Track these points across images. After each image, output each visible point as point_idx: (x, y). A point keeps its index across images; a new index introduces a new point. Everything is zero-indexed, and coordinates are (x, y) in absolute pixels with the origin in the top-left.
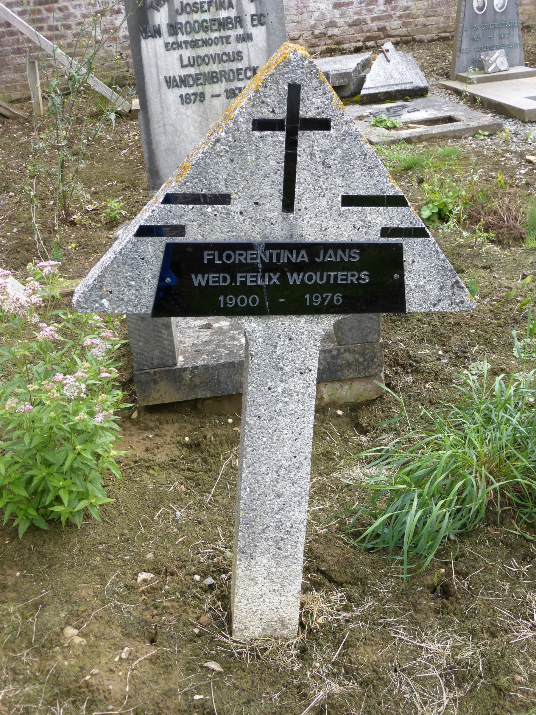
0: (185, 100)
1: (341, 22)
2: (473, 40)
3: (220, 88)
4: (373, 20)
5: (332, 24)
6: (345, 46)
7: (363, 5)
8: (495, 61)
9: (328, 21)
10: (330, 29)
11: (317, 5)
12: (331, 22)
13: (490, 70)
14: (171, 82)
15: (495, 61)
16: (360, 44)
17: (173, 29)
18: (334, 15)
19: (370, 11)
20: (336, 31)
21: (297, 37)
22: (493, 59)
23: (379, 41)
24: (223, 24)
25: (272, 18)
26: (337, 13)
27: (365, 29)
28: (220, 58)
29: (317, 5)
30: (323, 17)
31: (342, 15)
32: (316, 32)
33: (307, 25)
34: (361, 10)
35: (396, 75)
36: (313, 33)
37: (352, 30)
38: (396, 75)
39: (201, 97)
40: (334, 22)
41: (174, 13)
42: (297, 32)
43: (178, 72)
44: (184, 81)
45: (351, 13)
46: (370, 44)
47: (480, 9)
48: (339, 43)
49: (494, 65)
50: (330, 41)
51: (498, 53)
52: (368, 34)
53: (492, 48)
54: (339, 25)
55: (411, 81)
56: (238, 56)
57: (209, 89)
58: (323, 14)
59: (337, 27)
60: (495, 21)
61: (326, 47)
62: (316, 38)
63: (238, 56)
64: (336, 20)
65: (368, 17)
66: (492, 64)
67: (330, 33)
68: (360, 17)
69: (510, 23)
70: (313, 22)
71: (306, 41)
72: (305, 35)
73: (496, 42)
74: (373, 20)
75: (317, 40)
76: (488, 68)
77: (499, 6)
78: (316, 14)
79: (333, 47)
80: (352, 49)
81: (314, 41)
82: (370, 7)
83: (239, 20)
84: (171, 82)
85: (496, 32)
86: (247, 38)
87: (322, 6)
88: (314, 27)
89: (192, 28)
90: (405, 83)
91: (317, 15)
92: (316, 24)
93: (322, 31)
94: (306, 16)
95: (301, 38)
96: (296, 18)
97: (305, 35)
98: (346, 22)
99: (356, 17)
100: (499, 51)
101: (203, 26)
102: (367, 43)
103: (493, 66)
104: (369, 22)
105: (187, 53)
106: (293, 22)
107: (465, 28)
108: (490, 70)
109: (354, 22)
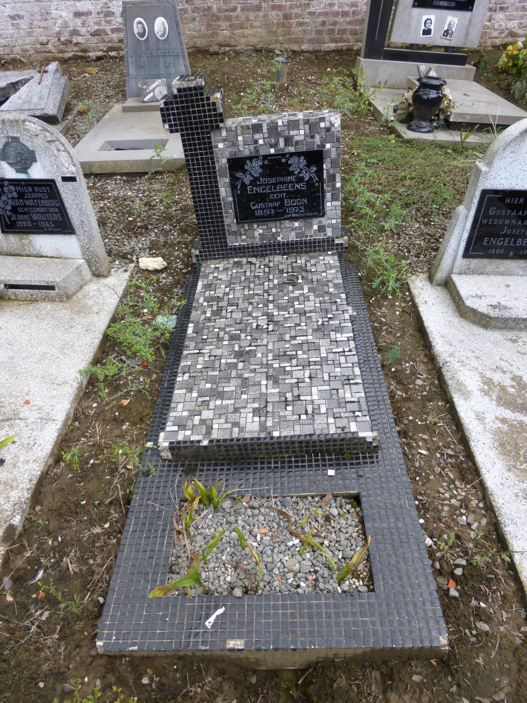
1: (83, 30)
2: (139, 67)
4: (113, 31)
5: (75, 32)
6: (90, 54)
7: (101, 16)
8: (153, 91)
9: (72, 29)
10: (74, 37)
11: (59, 13)
12: (74, 30)
13: (146, 99)
15: (153, 91)
16: (100, 54)
18: (76, 23)
19: (108, 22)
20: (80, 39)
21: (45, 42)
22: (151, 88)
23: (120, 52)
26: (78, 22)
27: (106, 40)
29: (59, 13)
30: (65, 25)
31: (83, 24)
32: (63, 39)
33: (53, 31)
34: (100, 21)
35: (35, 100)
36: (59, 39)
37: (95, 40)
38: (35, 100)
40: (77, 30)
42: (44, 37)
45: (92, 24)
46: (113, 54)
47: (142, 35)
48: (84, 51)
49: (151, 94)
50: (76, 49)
51: (158, 82)
52: (110, 44)
53: (157, 77)
54: (82, 33)
55: (43, 107)
58: (65, 22)
59: (80, 36)
60: (158, 49)
61: (74, 53)
62: (63, 44)
64: (79, 29)
65: (108, 28)
66: (150, 93)
67: (75, 41)
68: (100, 28)
69: (174, 52)
70: (58, 29)
71: (55, 46)
72: (53, 41)
73: (162, 70)
74: (113, 31)
75: (64, 46)
76: (145, 97)
77: (160, 33)
78: (60, 22)
79: (80, 54)
80: (94, 58)
81: (62, 47)
82: (108, 19)
85: (161, 60)
87: (64, 14)
88: (59, 34)
90: (37, 109)
91: (60, 22)
92: (60, 30)
93: (68, 38)
94: (50, 22)
95: (50, 43)
96: (42, 24)
97: (53, 41)
98: (88, 32)
99: (96, 28)
100: (160, 80)
102: (110, 53)
103: (151, 94)
104: (109, 33)
106: (40, 27)
107: (129, 55)
108: (146, 99)
109: (95, 31)
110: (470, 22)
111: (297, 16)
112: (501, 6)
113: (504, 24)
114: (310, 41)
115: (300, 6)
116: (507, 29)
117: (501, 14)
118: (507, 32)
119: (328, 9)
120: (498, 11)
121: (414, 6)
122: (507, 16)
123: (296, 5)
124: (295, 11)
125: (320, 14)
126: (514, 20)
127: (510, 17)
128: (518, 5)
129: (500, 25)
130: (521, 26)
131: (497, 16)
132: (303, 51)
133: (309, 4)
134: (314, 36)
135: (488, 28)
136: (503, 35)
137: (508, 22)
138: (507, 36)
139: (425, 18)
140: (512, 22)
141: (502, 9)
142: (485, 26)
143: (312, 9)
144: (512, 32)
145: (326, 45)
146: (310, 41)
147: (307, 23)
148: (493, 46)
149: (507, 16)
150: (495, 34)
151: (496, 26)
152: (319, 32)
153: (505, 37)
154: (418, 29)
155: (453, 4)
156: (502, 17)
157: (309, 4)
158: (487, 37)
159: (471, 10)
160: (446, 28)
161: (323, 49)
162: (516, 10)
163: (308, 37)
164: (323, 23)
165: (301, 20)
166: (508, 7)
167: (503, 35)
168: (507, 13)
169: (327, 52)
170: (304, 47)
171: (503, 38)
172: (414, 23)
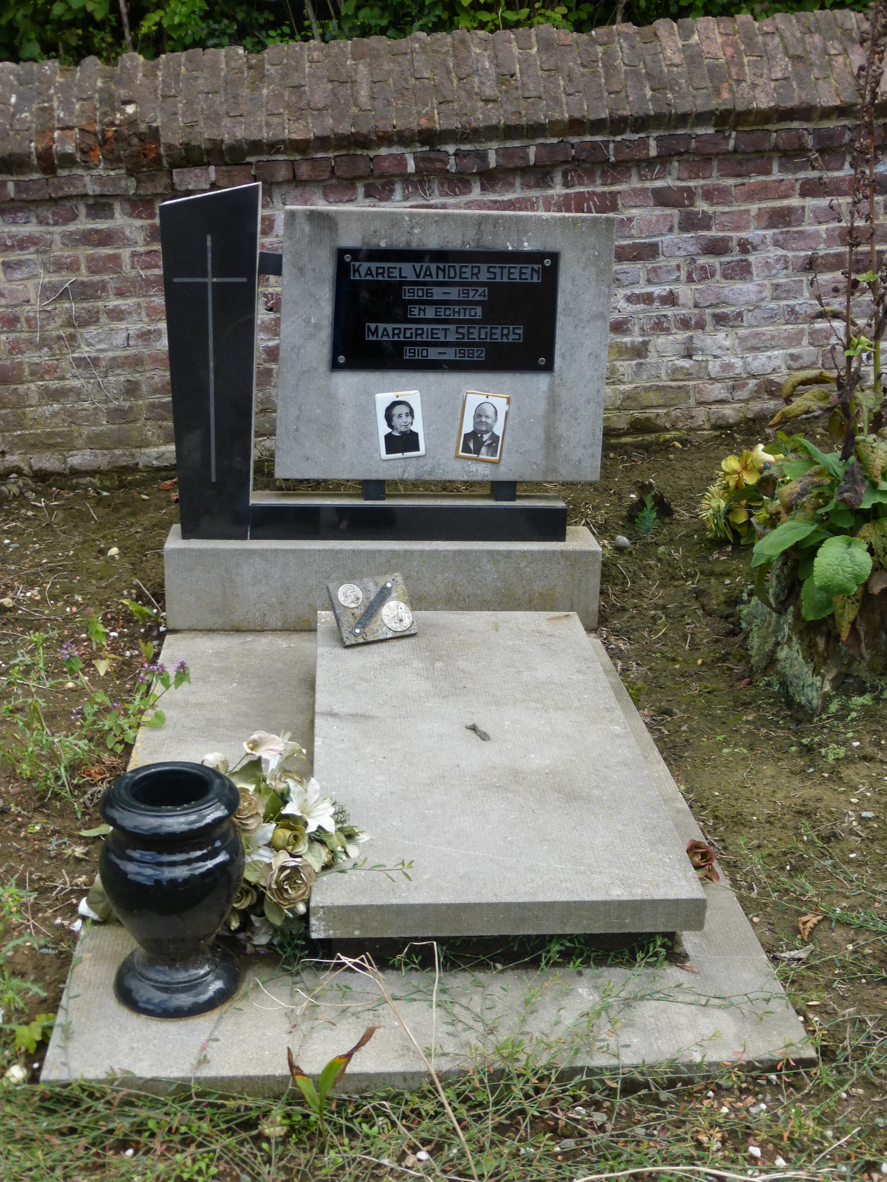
110: (553, 401)
111: (38, 373)
112: (718, 311)
113: (738, 363)
114: (95, 442)
115: (44, 343)
116: (754, 376)
117: (721, 335)
118: (752, 383)
119: (137, 349)
120: (709, 328)
121: (335, 366)
122: (742, 340)
123: (30, 342)
124: (30, 357)
125: (115, 364)
126: (767, 348)
127: (754, 342)
128: (773, 305)
129: (728, 367)
130: (795, 365)
131: (709, 341)
132: (75, 472)
133: (72, 337)
134: (104, 426)
135: (689, 375)
136: (743, 394)
137: (750, 357)
138: (756, 395)
139: (383, 399)
140: (762, 357)
141: (720, 320)
142: (676, 370)
143: (85, 351)
144: (771, 382)
145: (153, 451)
146: (95, 442)
147: (77, 393)
148: (715, 427)
149: (742, 340)
150: (717, 391)
151: (714, 368)
152: (119, 415)
153: (752, 398)
154: (367, 432)
155: (478, 355)
156: (727, 343)
157: (72, 337)
158: (692, 402)
159: (549, 368)
160: (468, 427)
161: (142, 462)
162: (771, 318)
163: (85, 431)
164: (131, 389)
165: (54, 384)
166: (740, 315)
167: (743, 394)
168: (742, 332)
169: (158, 469)
170: (79, 459)
171: (746, 401)
172: (347, 416)
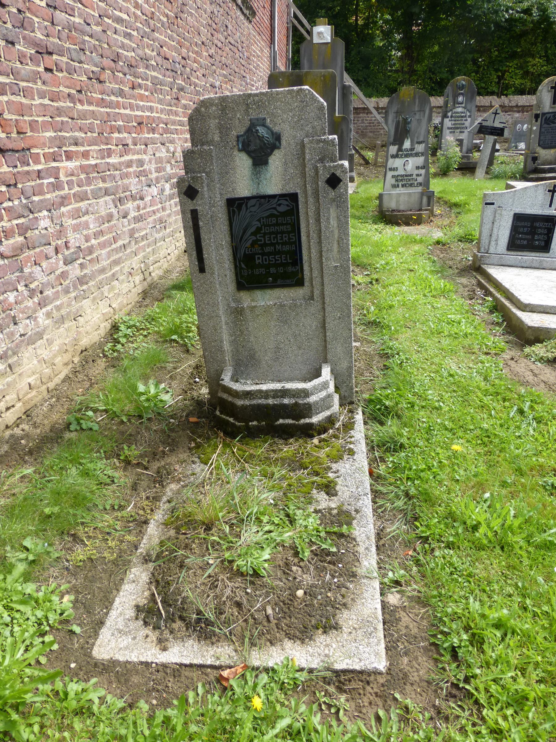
0: (451, 132)
3: (458, 130)
14: (448, 128)
17: (452, 117)
24: (462, 117)
25: (472, 116)
28: (460, 124)
39: (454, 132)
41: (452, 113)
43: (450, 126)
44: (451, 128)
53: (521, 142)
56: (464, 124)
57: (456, 131)
63: (464, 124)
83: (466, 116)
84: (448, 128)
86: (466, 120)
89: (455, 117)
101: (458, 117)
105: (453, 122)
